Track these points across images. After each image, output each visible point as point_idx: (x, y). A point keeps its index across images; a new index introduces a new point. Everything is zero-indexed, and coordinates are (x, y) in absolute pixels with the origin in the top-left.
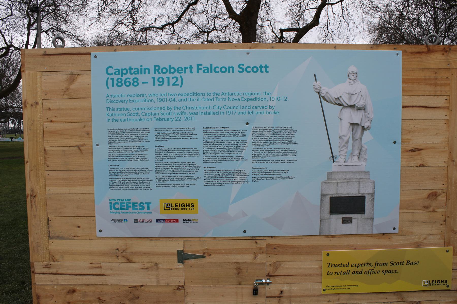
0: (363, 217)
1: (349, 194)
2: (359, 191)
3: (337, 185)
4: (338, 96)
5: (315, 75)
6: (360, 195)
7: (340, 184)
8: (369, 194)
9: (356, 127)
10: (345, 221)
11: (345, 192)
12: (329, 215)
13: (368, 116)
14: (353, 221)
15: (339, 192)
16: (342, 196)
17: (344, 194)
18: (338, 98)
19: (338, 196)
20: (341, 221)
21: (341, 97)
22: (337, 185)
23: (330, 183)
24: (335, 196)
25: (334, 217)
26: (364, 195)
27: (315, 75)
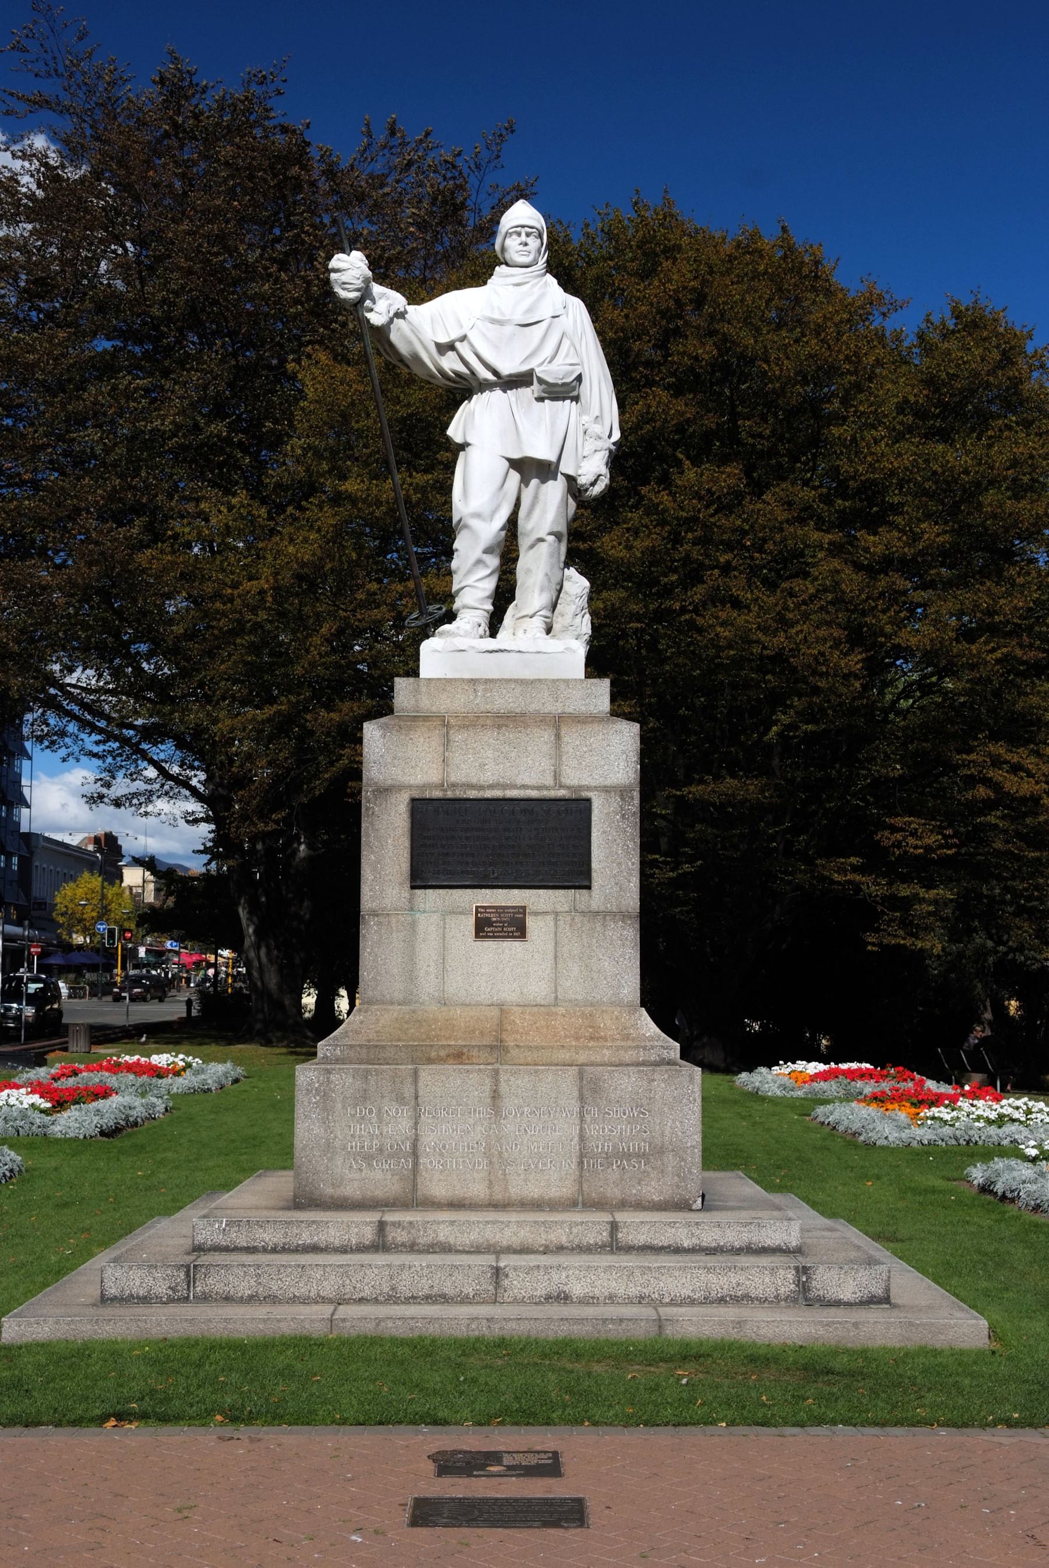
0: (582, 907)
1: (505, 787)
2: (557, 775)
3: (447, 743)
4: (454, 335)
6: (562, 793)
7: (458, 737)
8: (606, 790)
10: (486, 926)
11: (488, 776)
12: (406, 892)
14: (532, 923)
16: (472, 794)
17: (481, 788)
19: (450, 794)
21: (463, 338)
22: (447, 743)
24: (437, 794)
25: (431, 898)
26: (585, 794)
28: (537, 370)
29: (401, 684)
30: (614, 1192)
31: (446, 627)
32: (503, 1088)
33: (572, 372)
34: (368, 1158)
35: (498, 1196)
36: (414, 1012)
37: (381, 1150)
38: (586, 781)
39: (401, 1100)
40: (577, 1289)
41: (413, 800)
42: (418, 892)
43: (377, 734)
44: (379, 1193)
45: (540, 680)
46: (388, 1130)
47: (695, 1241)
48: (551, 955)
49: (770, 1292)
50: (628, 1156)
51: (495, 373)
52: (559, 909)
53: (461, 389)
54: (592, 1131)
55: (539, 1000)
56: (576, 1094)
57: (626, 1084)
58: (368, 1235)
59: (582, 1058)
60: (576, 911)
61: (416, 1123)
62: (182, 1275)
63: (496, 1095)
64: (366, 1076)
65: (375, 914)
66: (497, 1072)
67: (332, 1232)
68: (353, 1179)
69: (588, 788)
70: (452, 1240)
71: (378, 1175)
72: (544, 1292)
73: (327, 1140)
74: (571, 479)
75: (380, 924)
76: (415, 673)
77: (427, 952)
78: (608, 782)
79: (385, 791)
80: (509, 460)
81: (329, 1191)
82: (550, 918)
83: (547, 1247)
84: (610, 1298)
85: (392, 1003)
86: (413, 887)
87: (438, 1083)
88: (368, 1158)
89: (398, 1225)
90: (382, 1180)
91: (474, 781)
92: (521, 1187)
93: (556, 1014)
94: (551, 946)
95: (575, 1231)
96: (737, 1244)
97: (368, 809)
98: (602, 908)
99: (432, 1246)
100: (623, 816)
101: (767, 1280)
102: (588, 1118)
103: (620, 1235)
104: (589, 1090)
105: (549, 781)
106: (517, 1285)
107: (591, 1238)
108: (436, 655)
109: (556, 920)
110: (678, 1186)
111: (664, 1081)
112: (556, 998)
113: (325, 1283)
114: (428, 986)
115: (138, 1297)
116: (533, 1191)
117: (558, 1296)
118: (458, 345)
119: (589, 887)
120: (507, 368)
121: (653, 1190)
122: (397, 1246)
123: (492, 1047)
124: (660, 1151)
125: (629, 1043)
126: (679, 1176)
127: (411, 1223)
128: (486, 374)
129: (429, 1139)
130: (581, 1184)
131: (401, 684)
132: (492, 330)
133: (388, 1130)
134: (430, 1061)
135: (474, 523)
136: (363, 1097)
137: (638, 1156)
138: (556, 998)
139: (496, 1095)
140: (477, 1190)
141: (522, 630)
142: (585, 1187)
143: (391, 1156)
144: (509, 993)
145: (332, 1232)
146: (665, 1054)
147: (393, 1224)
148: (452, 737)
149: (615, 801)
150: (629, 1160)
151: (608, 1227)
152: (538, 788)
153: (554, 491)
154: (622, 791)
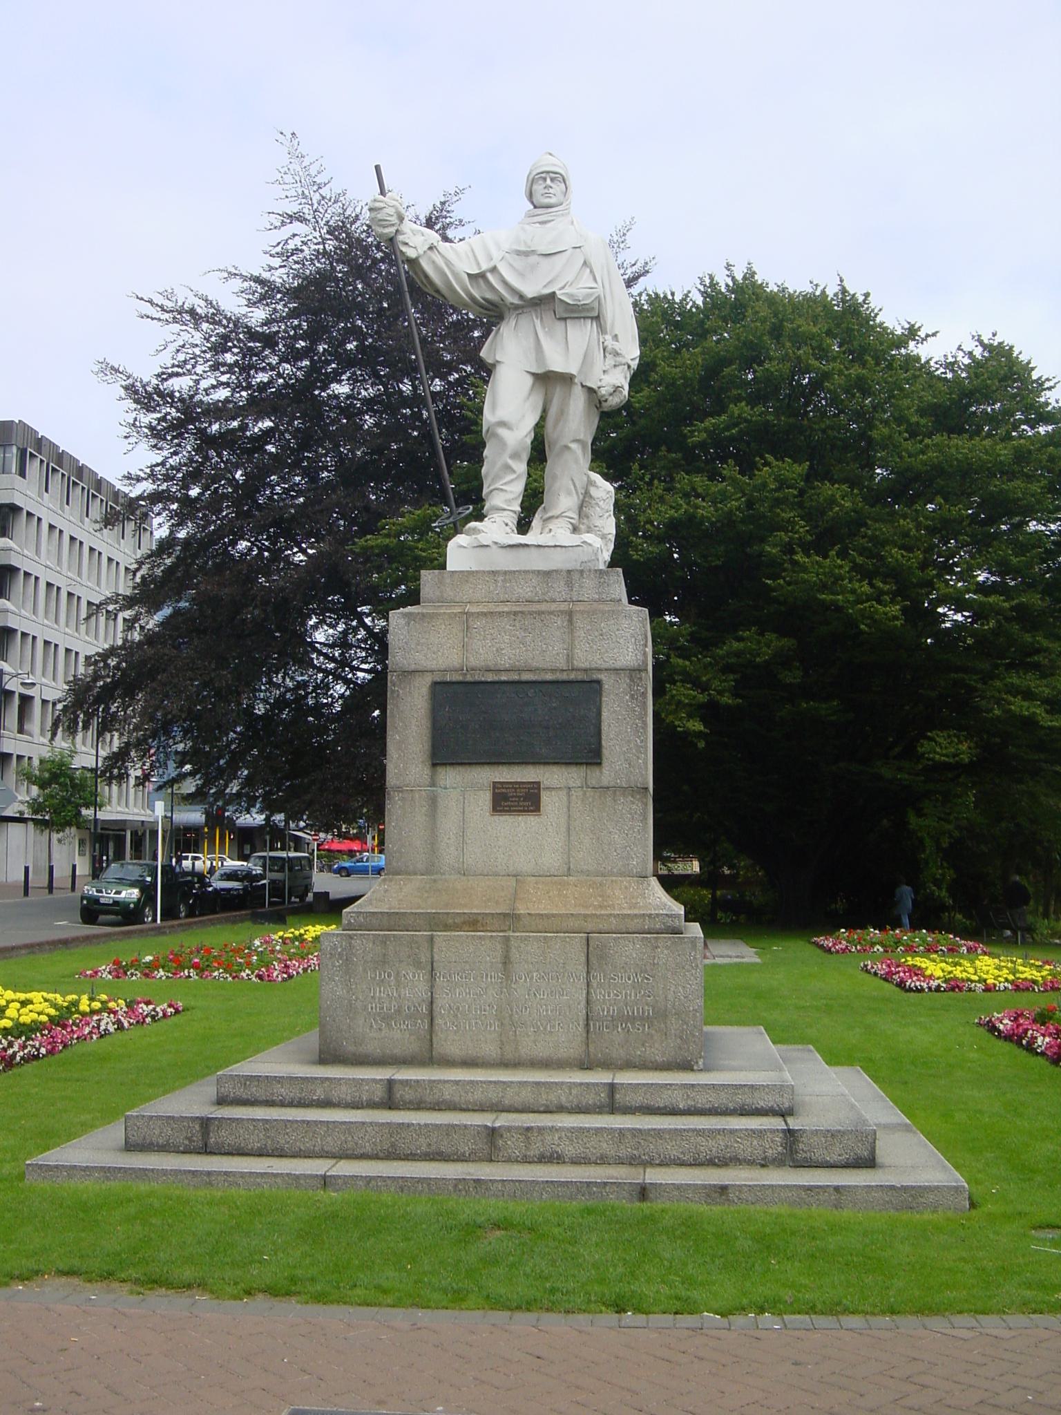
0: (593, 782)
1: (519, 671)
2: (570, 658)
4: (484, 267)
5: (377, 168)
8: (616, 670)
9: (558, 392)
11: (505, 662)
12: (427, 771)
13: (610, 343)
14: (545, 797)
15: (473, 662)
16: (490, 677)
18: (482, 276)
19: (469, 678)
20: (486, 798)
21: (494, 270)
23: (433, 616)
24: (457, 677)
25: (451, 777)
26: (596, 676)
27: (377, 168)
28: (558, 292)
29: (427, 576)
30: (618, 1053)
31: (473, 524)
32: (515, 955)
33: (591, 295)
34: (386, 1018)
35: (509, 1056)
36: (435, 881)
37: (399, 1011)
38: (600, 663)
39: (418, 964)
40: (569, 1150)
41: (435, 684)
42: (440, 769)
43: (402, 621)
44: (397, 1051)
45: (556, 571)
46: (406, 992)
47: (690, 1102)
48: (563, 829)
49: (758, 1153)
50: (632, 1019)
51: (521, 297)
52: (571, 784)
53: (494, 314)
54: (597, 995)
55: (553, 871)
56: (583, 959)
57: (631, 950)
58: (379, 1093)
59: (590, 926)
60: (588, 787)
61: (432, 987)
62: (197, 1127)
63: (506, 961)
64: (384, 941)
65: (399, 789)
66: (507, 939)
67: (344, 1088)
68: (375, 1039)
69: (599, 670)
70: (457, 1099)
71: (397, 1035)
72: (537, 1152)
73: (350, 1001)
74: (591, 391)
75: (403, 799)
76: (440, 564)
77: (448, 824)
78: (618, 665)
79: (409, 674)
80: (533, 374)
81: (351, 1048)
82: (563, 794)
83: (547, 1106)
84: (602, 1158)
85: (415, 874)
86: (434, 765)
87: (449, 946)
88: (386, 1018)
89: (406, 1083)
90: (401, 1038)
91: (491, 664)
92: (529, 1047)
93: (569, 884)
94: (563, 820)
95: (574, 1092)
96: (731, 1106)
97: (393, 692)
98: (612, 784)
99: (438, 1103)
100: (632, 696)
101: (755, 1142)
102: (594, 983)
103: (618, 1096)
104: (593, 957)
105: (561, 663)
106: (513, 1145)
107: (590, 1099)
108: (460, 552)
109: (569, 796)
110: (680, 1048)
111: (667, 948)
112: (569, 869)
113: (329, 1139)
114: (449, 854)
115: (158, 1145)
116: (542, 1050)
117: (551, 1156)
118: (489, 276)
119: (600, 764)
120: (531, 291)
121: (657, 1052)
122: (405, 1103)
123: (505, 915)
124: (661, 1015)
125: (636, 912)
126: (681, 1038)
127: (418, 1081)
128: (511, 299)
129: (442, 1001)
130: (588, 1045)
131: (427, 576)
132: (519, 263)
133: (406, 992)
134: (447, 928)
135: (502, 432)
136: (383, 961)
137: (642, 1019)
138: (569, 869)
139: (506, 961)
140: (490, 1049)
141: (552, 532)
142: (592, 1049)
143: (409, 1017)
144: (524, 863)
145: (344, 1088)
146: (670, 922)
147: (401, 1082)
148: (471, 623)
149: (624, 681)
150: (633, 1024)
151: (607, 1088)
152: (553, 671)
153: (577, 403)
154: (634, 672)
